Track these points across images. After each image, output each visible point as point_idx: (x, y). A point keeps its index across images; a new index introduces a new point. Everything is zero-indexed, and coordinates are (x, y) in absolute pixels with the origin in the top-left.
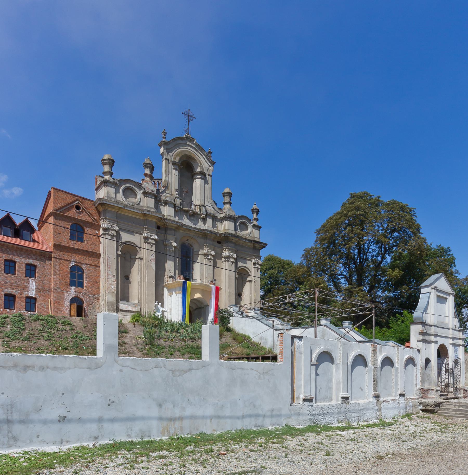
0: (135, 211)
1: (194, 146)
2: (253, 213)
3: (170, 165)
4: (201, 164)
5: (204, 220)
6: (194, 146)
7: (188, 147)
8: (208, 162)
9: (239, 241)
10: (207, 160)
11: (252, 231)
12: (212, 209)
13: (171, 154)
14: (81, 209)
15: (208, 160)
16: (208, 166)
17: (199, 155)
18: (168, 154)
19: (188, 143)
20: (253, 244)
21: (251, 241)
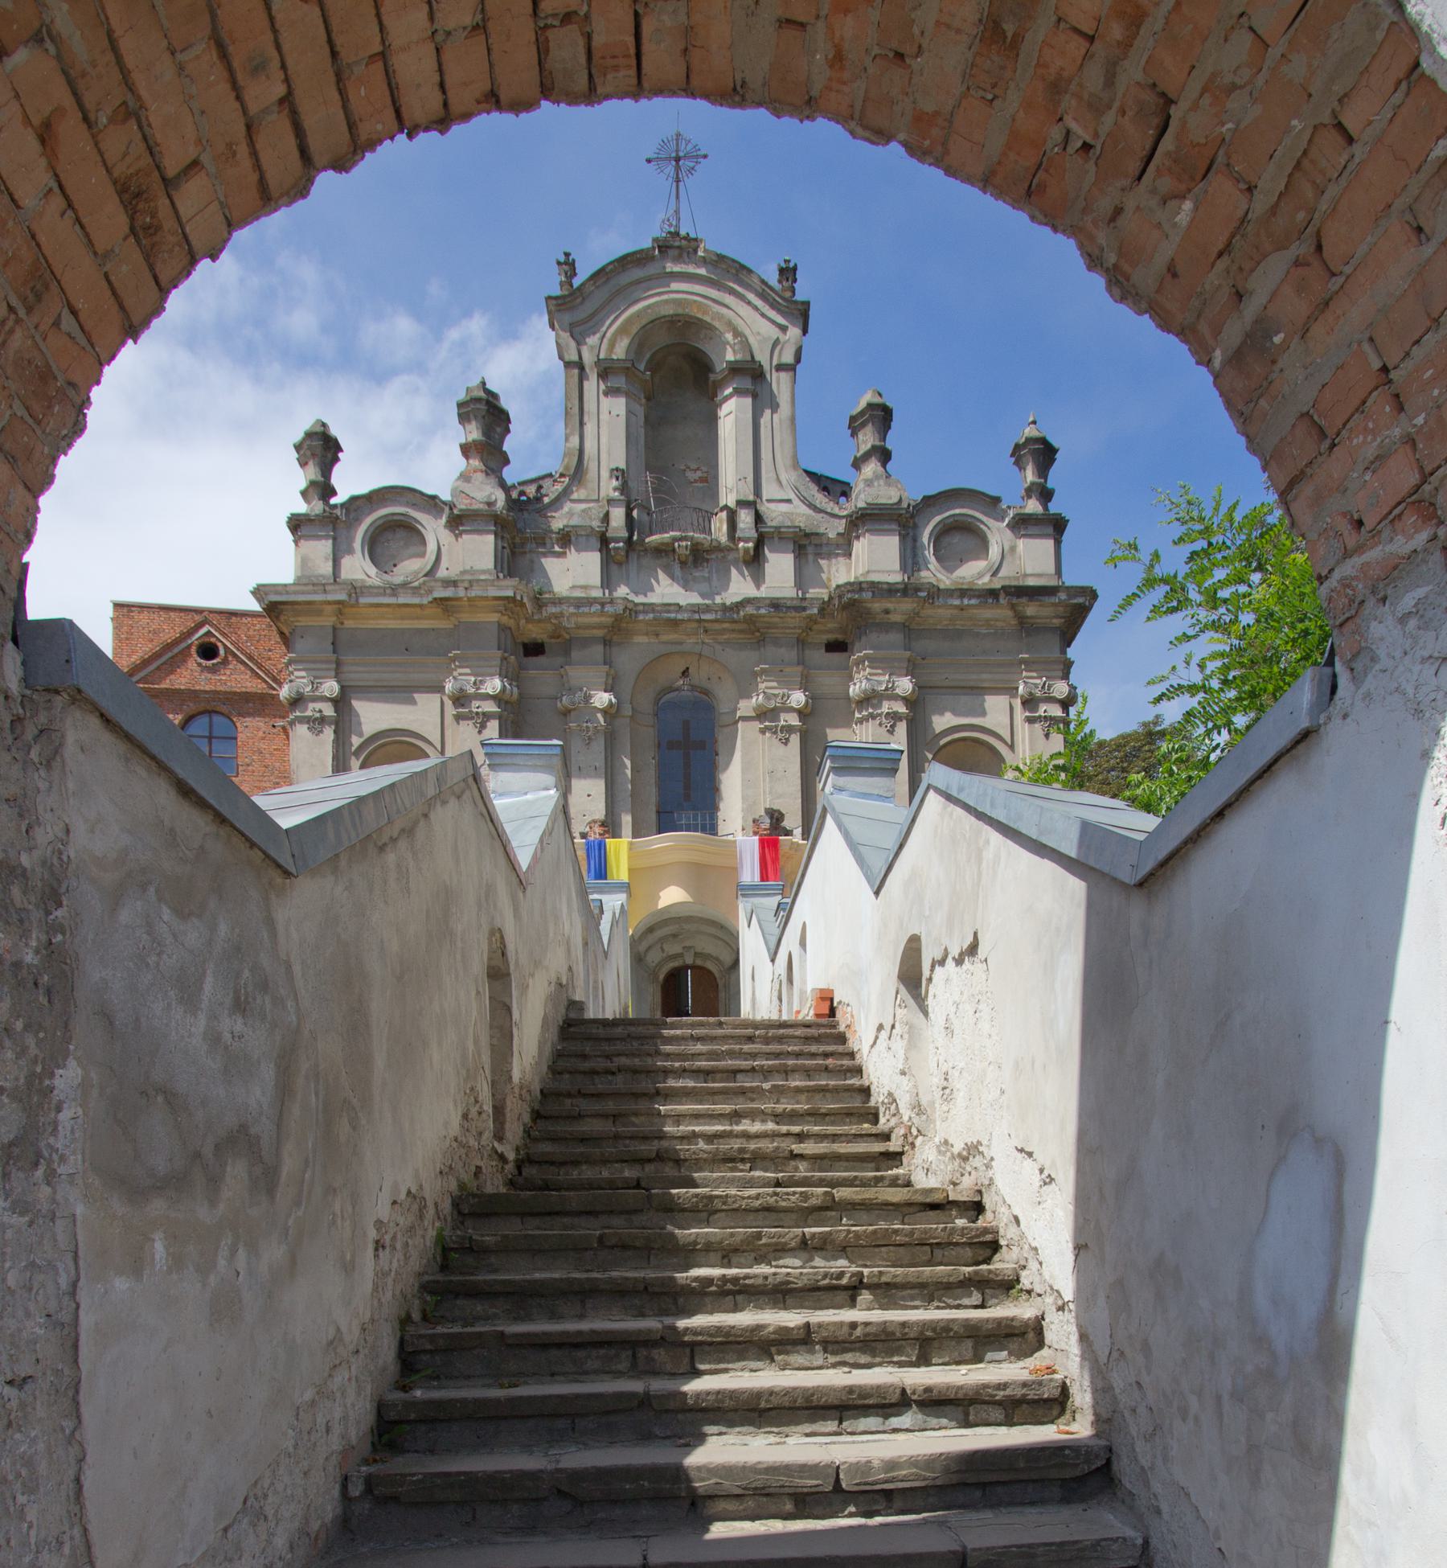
0: (401, 600)
1: (702, 271)
2: (1019, 464)
3: (592, 385)
4: (737, 333)
5: (755, 561)
6: (702, 271)
7: (674, 286)
8: (772, 314)
9: (928, 611)
10: (759, 303)
11: (1013, 549)
13: (593, 340)
14: (222, 652)
15: (774, 306)
16: (775, 333)
17: (729, 299)
18: (579, 344)
19: (671, 267)
20: (1013, 607)
21: (993, 593)
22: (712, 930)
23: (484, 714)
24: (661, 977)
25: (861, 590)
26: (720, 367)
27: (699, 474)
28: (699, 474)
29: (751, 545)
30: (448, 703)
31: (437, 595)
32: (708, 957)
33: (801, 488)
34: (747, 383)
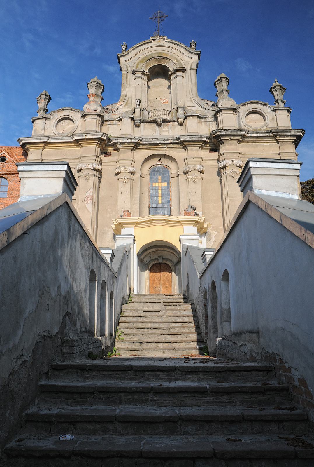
12: (200, 108)
22: (170, 250)
25: (221, 132)
26: (172, 70)
27: (165, 101)
28: (165, 101)
31: (76, 138)
32: (168, 260)
33: (199, 103)
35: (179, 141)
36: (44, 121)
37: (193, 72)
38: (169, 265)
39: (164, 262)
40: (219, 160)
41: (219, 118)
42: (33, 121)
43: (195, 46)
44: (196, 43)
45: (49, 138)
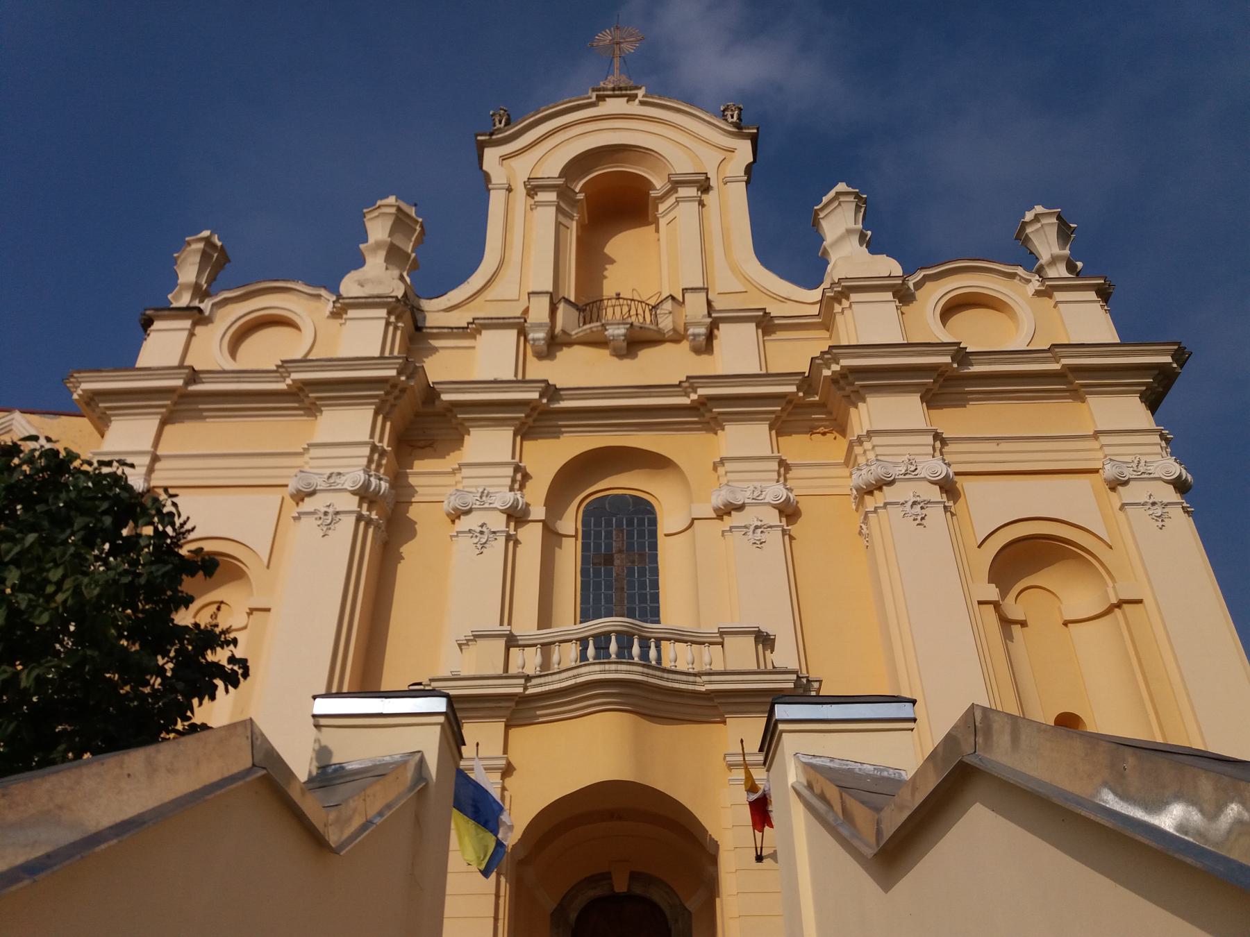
23: (337, 513)
24: (573, 916)
29: (702, 330)
30: (289, 502)
34: (692, 192)
35: (694, 397)
36: (187, 324)
37: (738, 193)
38: (655, 907)
39: (638, 890)
40: (849, 460)
41: (839, 318)
42: (147, 323)
43: (739, 118)
44: (740, 109)
45: (194, 376)
